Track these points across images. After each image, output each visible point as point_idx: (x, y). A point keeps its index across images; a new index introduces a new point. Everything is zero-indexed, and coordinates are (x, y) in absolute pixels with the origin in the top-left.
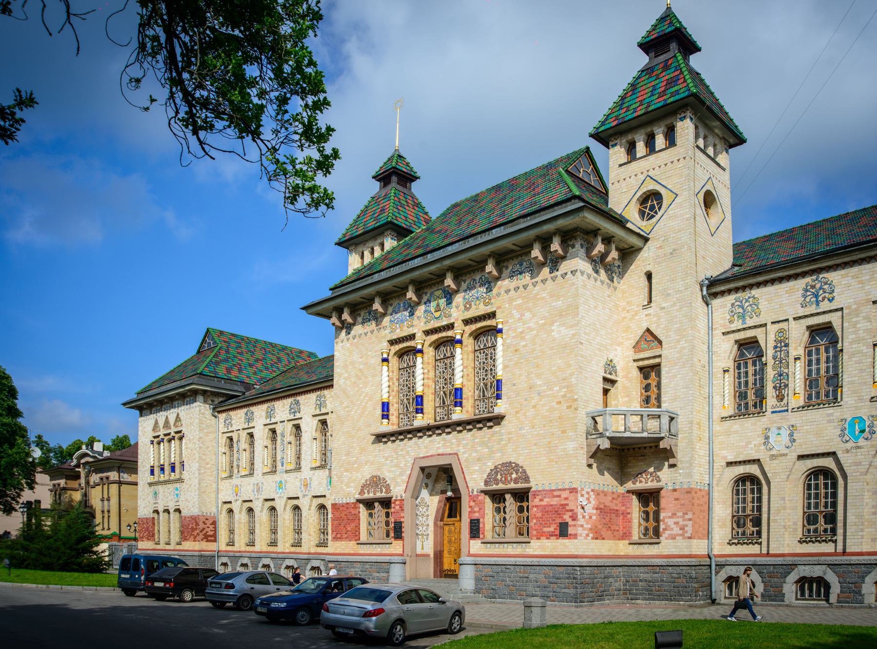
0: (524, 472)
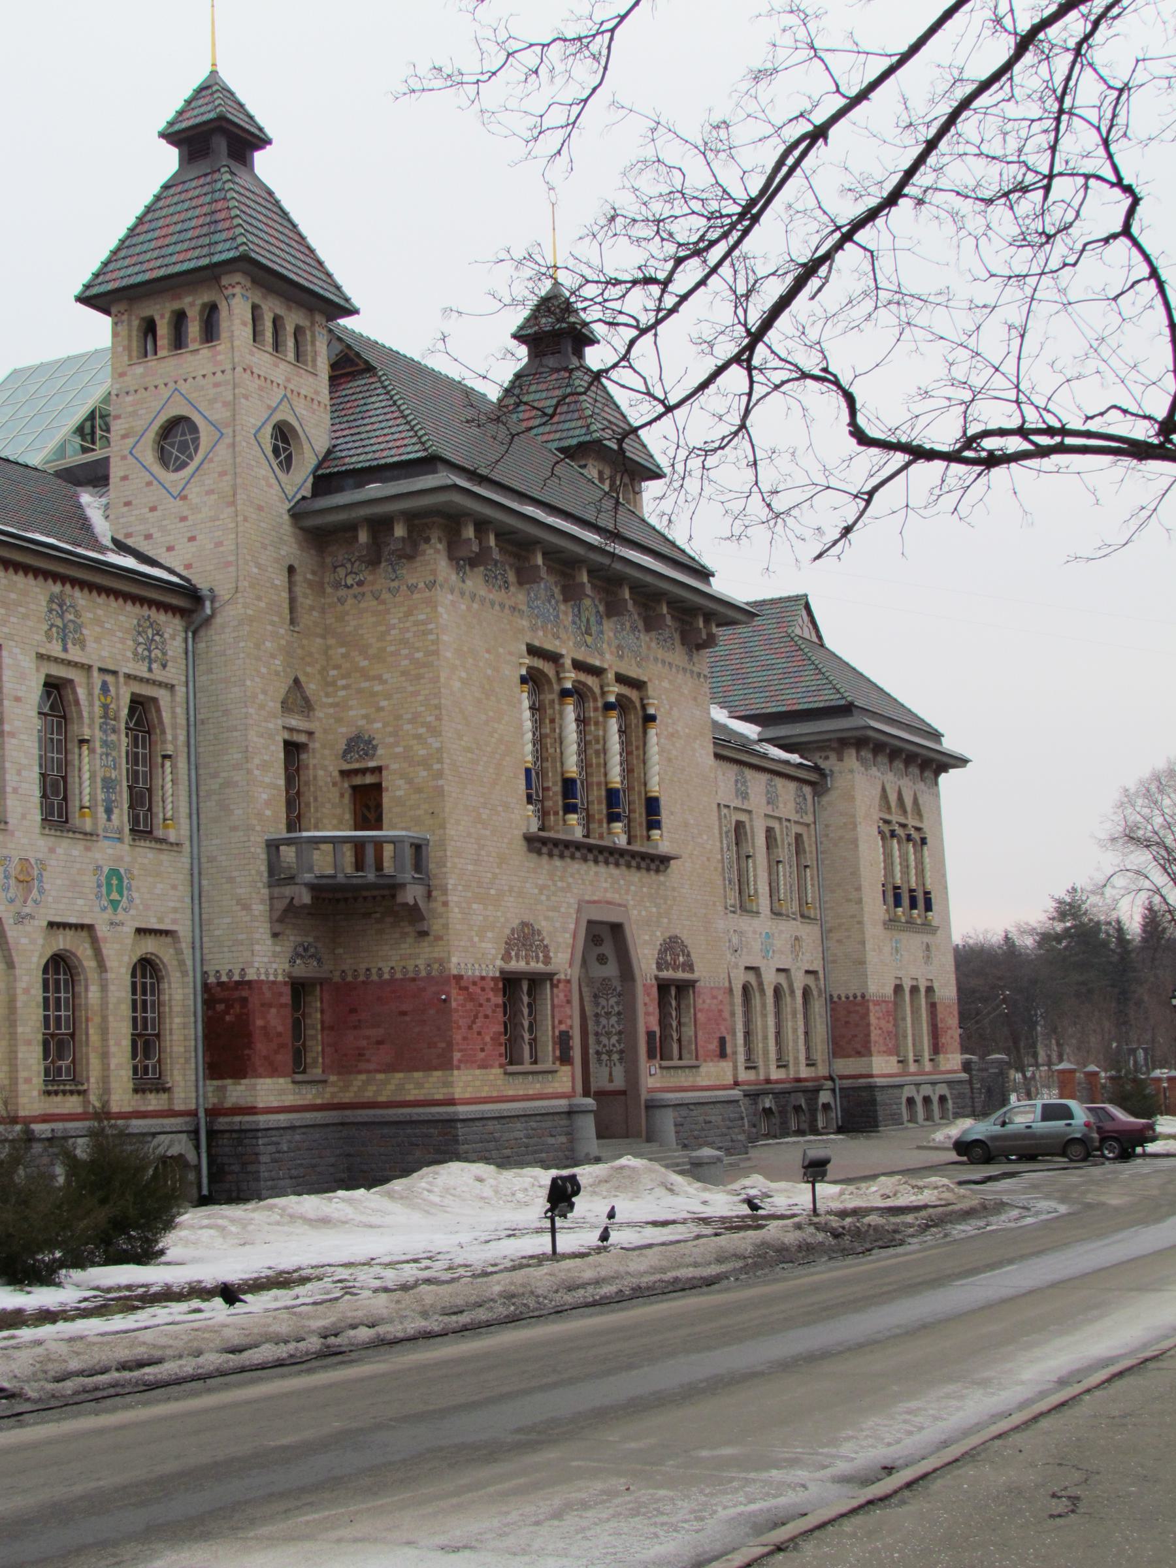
0: (689, 955)
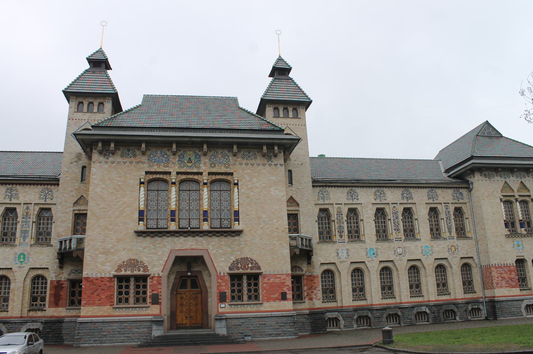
0: (257, 263)
